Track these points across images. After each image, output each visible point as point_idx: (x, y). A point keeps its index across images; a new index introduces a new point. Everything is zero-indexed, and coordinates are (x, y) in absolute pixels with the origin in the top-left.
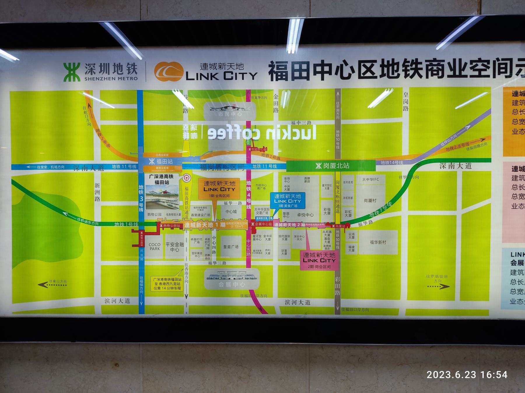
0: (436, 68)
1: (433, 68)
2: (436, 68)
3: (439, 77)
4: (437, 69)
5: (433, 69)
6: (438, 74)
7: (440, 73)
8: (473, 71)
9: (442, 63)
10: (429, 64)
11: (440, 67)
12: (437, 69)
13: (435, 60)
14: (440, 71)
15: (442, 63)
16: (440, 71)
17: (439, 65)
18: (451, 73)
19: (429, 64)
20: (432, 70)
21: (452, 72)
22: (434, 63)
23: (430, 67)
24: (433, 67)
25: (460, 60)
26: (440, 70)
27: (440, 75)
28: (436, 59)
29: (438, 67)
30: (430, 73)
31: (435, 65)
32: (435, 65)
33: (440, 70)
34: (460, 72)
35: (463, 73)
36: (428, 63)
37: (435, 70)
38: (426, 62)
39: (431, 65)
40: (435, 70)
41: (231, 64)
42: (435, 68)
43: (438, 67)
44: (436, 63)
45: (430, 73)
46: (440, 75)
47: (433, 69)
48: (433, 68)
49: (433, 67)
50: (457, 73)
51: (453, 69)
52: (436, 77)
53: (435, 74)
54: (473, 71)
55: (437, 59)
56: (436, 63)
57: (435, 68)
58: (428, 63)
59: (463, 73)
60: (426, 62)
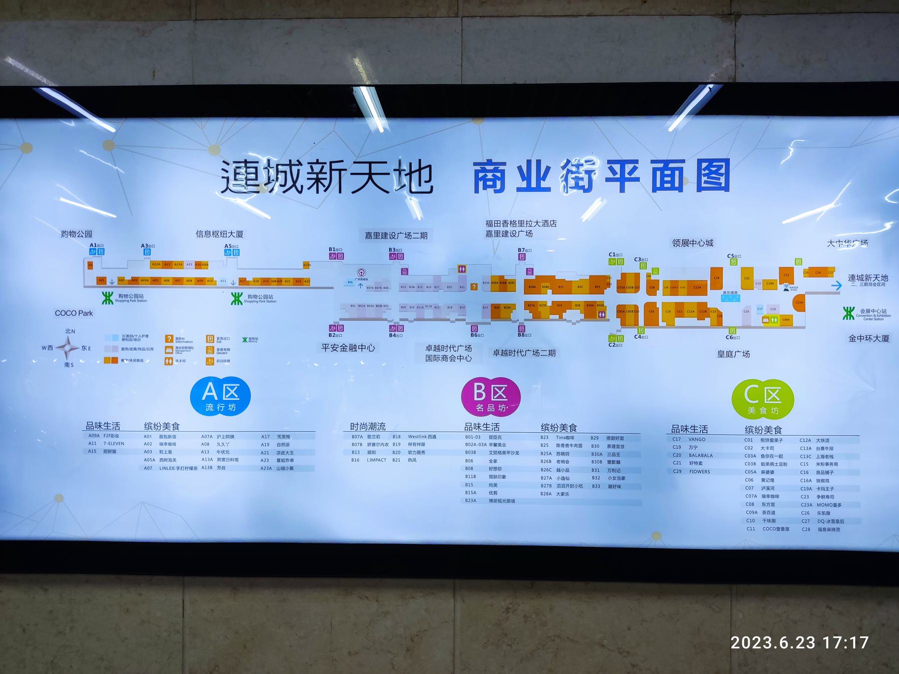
0: (492, 176)
1: (487, 176)
2: (492, 176)
3: (496, 192)
4: (493, 178)
5: (487, 178)
6: (494, 186)
7: (498, 183)
8: (544, 180)
9: (501, 168)
10: (480, 169)
11: (499, 175)
12: (493, 178)
13: (489, 162)
14: (497, 181)
15: (501, 168)
16: (497, 181)
17: (496, 170)
18: (524, 184)
19: (480, 169)
20: (484, 179)
21: (525, 182)
22: (488, 168)
23: (481, 175)
24: (487, 174)
25: (539, 162)
26: (499, 179)
27: (498, 187)
28: (491, 160)
29: (495, 173)
30: (481, 183)
31: (490, 171)
32: (490, 171)
33: (499, 179)
34: (538, 183)
35: (543, 184)
36: (478, 168)
37: (490, 180)
38: (474, 165)
39: (484, 170)
40: (490, 180)
41: (370, 163)
42: (490, 176)
43: (495, 173)
44: (491, 168)
45: (481, 183)
46: (498, 187)
47: (487, 178)
48: (487, 176)
49: (487, 174)
50: (534, 185)
51: (526, 177)
52: (491, 190)
53: (490, 187)
54: (544, 180)
55: (493, 161)
56: (491, 168)
57: (490, 176)
58: (478, 168)
59: (543, 184)
60: (474, 165)
